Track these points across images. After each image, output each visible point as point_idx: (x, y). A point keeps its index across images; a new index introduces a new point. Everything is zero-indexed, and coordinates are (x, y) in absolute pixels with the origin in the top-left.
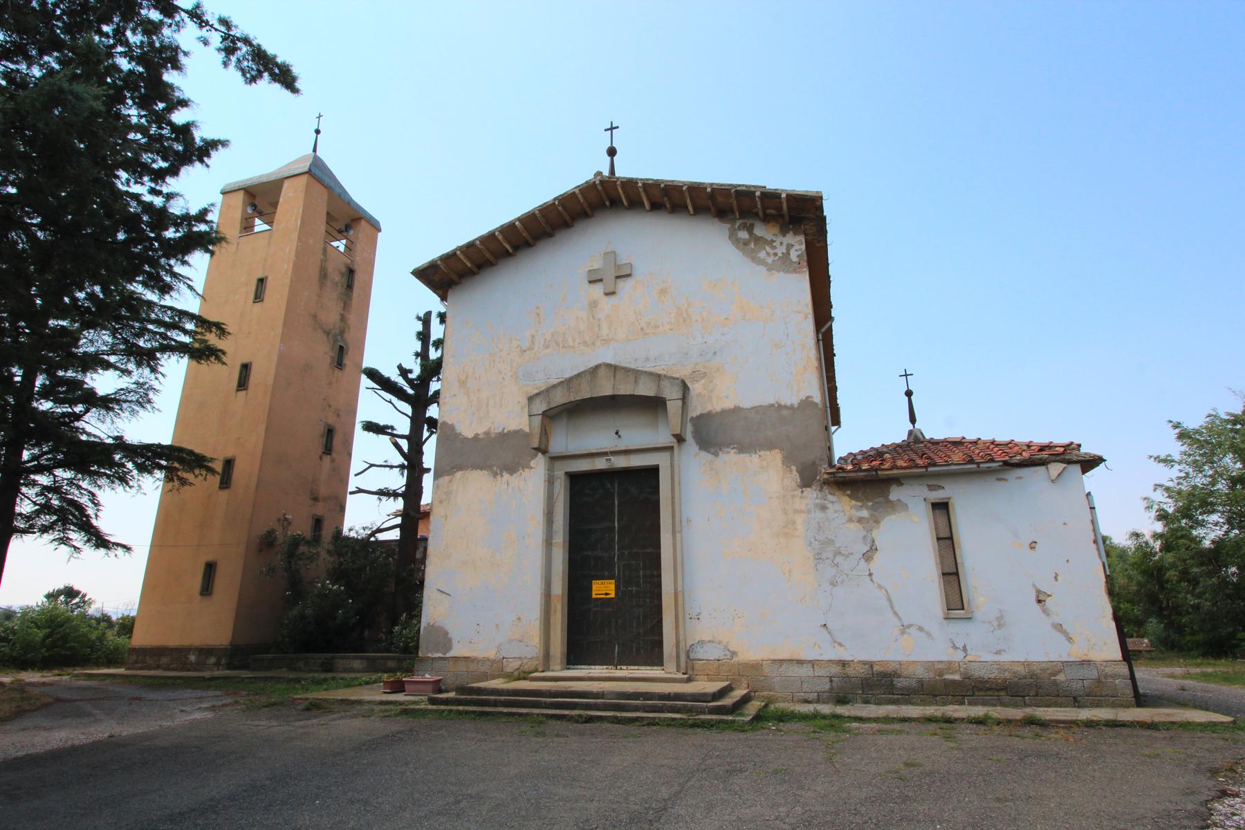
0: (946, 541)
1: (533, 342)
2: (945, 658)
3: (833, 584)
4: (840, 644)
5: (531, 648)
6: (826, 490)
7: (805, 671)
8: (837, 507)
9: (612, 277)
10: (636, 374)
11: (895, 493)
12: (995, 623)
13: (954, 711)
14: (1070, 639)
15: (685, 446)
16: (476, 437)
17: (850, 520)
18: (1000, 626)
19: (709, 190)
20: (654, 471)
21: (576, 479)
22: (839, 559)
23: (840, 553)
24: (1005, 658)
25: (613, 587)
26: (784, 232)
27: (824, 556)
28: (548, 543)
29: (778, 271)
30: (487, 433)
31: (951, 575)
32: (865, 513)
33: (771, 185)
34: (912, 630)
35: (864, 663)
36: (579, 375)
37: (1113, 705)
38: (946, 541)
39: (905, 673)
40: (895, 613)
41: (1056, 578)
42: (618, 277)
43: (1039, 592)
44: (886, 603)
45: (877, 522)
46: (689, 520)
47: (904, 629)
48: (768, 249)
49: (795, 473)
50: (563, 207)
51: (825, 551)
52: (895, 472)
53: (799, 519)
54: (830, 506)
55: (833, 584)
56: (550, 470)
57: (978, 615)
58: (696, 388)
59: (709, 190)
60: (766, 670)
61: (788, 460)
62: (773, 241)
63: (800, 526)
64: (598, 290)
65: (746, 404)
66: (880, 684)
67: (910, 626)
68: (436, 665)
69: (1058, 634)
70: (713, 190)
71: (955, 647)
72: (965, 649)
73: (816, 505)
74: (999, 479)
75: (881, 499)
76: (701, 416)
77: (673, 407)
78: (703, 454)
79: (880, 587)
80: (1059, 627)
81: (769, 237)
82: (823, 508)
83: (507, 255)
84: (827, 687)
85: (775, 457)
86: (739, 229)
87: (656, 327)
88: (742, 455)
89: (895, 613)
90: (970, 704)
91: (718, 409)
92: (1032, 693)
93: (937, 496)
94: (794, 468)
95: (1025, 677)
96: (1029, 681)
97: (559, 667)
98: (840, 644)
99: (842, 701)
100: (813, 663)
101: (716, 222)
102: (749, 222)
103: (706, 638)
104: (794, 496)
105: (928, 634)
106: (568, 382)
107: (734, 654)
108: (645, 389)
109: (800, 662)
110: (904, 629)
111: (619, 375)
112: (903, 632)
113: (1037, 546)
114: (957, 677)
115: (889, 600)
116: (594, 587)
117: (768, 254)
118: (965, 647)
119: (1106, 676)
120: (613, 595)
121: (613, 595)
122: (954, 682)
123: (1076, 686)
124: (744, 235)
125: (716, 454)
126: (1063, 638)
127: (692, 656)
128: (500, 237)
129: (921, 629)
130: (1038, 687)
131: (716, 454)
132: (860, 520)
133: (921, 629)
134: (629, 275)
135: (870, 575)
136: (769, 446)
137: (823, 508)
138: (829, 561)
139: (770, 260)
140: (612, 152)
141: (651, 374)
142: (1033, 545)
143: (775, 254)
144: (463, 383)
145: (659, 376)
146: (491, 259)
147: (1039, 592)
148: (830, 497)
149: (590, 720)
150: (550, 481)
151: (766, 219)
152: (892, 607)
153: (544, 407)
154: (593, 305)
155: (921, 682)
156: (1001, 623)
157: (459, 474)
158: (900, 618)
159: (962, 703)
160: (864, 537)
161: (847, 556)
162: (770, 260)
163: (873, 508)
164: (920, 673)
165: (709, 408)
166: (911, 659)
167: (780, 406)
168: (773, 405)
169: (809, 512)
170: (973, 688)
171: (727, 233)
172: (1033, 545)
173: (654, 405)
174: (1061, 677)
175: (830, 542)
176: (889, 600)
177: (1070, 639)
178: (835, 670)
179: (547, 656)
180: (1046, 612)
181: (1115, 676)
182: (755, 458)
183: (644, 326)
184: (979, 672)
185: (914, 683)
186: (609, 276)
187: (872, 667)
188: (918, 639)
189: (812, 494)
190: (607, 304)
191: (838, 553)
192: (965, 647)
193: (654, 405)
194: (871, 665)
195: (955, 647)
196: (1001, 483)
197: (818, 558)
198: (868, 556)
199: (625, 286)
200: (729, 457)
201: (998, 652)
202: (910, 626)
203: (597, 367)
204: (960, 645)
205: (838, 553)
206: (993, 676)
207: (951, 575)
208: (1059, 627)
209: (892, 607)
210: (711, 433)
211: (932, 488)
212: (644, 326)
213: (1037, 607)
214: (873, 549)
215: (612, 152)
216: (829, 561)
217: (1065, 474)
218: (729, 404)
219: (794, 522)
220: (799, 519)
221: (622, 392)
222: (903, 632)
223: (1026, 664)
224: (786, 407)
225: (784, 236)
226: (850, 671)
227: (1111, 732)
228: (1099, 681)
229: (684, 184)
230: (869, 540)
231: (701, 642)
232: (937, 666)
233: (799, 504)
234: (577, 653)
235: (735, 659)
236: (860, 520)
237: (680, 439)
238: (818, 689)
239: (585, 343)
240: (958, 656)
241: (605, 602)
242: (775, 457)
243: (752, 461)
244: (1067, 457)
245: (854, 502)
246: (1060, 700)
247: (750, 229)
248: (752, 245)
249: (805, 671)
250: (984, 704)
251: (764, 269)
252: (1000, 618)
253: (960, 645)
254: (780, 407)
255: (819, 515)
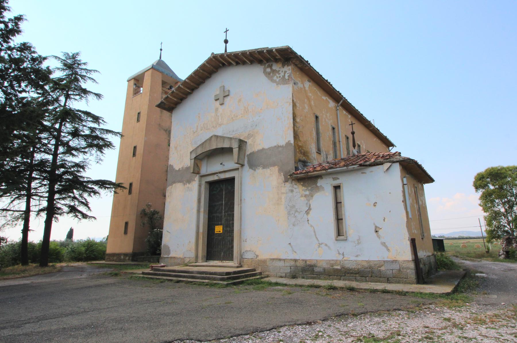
0: (338, 204)
1: (197, 129)
2: (335, 259)
3: (294, 225)
4: (295, 252)
5: (192, 255)
6: (294, 183)
7: (281, 264)
8: (297, 190)
9: (223, 96)
10: (223, 138)
11: (320, 183)
12: (356, 242)
13: (357, 285)
14: (388, 250)
15: (245, 167)
16: (179, 170)
17: (302, 196)
18: (359, 243)
19: (248, 53)
20: (232, 180)
21: (212, 185)
22: (297, 214)
23: (297, 211)
24: (359, 259)
25: (222, 228)
26: (283, 66)
27: (291, 213)
28: (199, 211)
29: (280, 84)
30: (182, 168)
31: (339, 220)
32: (307, 193)
33: (270, 46)
34: (323, 245)
35: (303, 260)
36: (206, 141)
37: (405, 283)
38: (338, 204)
39: (318, 265)
40: (317, 238)
41: (384, 220)
42: (225, 97)
43: (376, 227)
44: (313, 233)
45: (312, 196)
46: (244, 199)
47: (320, 245)
48: (277, 74)
49: (282, 176)
50: (202, 70)
51: (292, 210)
52: (315, 173)
53: (283, 196)
54: (294, 190)
55: (294, 225)
56: (200, 181)
57: (349, 238)
58: (249, 141)
59: (248, 53)
60: (268, 263)
61: (280, 170)
62: (279, 71)
63: (283, 200)
64: (218, 103)
65: (266, 147)
66: (308, 270)
67: (322, 244)
68: (166, 260)
69: (384, 247)
70: (267, 51)
71: (339, 254)
72: (343, 254)
73: (289, 190)
74: (363, 173)
75: (314, 186)
76: (251, 154)
77: (236, 151)
78: (251, 170)
79: (311, 226)
80: (384, 244)
81: (278, 69)
82: (292, 191)
83: (189, 94)
84: (289, 271)
85: (276, 169)
86: (267, 67)
87: (237, 116)
88: (264, 170)
89: (317, 238)
90: (343, 280)
91: (256, 150)
92: (370, 275)
93: (336, 183)
94: (282, 174)
95: (367, 268)
96: (369, 270)
97: (200, 261)
98: (295, 252)
99: (294, 277)
100: (284, 260)
101: (259, 65)
102: (270, 64)
103: (248, 249)
104: (281, 187)
105: (329, 247)
106: (202, 144)
107: (257, 256)
108: (226, 145)
109: (280, 260)
110: (320, 245)
111: (219, 139)
112: (319, 247)
113: (377, 205)
114: (339, 267)
115: (315, 232)
116: (216, 228)
117: (277, 77)
118: (343, 253)
119: (403, 268)
120: (221, 232)
121: (221, 232)
122: (337, 269)
123: (389, 273)
124: (269, 70)
125: (255, 170)
126: (386, 249)
127: (244, 257)
128: (182, 87)
129: (326, 245)
130: (372, 272)
131: (255, 170)
132: (305, 196)
133: (326, 245)
134: (228, 95)
135: (308, 220)
136: (274, 165)
137: (292, 191)
138: (293, 215)
139: (277, 80)
140: (226, 42)
141: (229, 138)
142: (375, 204)
143: (280, 77)
144: (176, 148)
145: (231, 138)
146: (184, 96)
147: (376, 227)
148: (295, 186)
149: (178, 282)
150: (200, 186)
151: (276, 61)
152: (315, 235)
153: (195, 156)
154: (217, 109)
155: (324, 269)
156: (359, 242)
157: (174, 185)
158: (318, 240)
159: (340, 279)
160: (307, 204)
161: (299, 212)
162: (277, 80)
163: (311, 190)
164: (325, 265)
165: (253, 150)
166: (321, 259)
167: (278, 146)
168: (276, 146)
169: (287, 193)
170: (345, 273)
171: (263, 70)
172: (375, 204)
173: (226, 151)
174: (383, 268)
175: (294, 206)
176: (315, 232)
177: (388, 250)
178: (292, 263)
179: (197, 257)
180: (379, 237)
181: (408, 268)
182: (268, 170)
183: (233, 116)
184: (348, 265)
185: (321, 270)
186: (221, 98)
187: (306, 262)
188: (325, 251)
189: (288, 185)
190: (221, 108)
191: (297, 211)
192: (343, 253)
193: (226, 151)
194: (306, 261)
195: (339, 254)
196: (364, 174)
197: (289, 214)
198: (307, 212)
199: (227, 100)
200: (260, 171)
201: (357, 256)
202: (322, 244)
203: (212, 137)
204: (341, 252)
205: (297, 211)
206: (353, 267)
207: (339, 220)
208: (384, 244)
209: (315, 235)
210: (255, 161)
211: (334, 179)
212: (233, 116)
213: (375, 234)
214: (310, 209)
215: (226, 42)
216: (293, 215)
217: (391, 168)
218: (260, 148)
219: (281, 198)
220: (283, 196)
221: (219, 147)
222: (319, 247)
223: (367, 262)
224: (280, 146)
225: (283, 67)
226: (298, 264)
227: (349, 293)
228: (399, 270)
229: (218, 54)
230: (308, 205)
231: (247, 251)
232: (331, 262)
233: (284, 190)
234: (210, 256)
235: (258, 258)
236: (305, 196)
237: (242, 165)
238: (286, 272)
239: (213, 127)
240: (340, 258)
241: (219, 235)
242: (276, 169)
243: (267, 171)
244: (392, 159)
245: (304, 188)
246: (381, 279)
247: (271, 67)
248: (271, 74)
249: (281, 264)
250: (349, 280)
251: (275, 84)
252: (358, 240)
253: (341, 252)
254: (278, 147)
255: (290, 194)
